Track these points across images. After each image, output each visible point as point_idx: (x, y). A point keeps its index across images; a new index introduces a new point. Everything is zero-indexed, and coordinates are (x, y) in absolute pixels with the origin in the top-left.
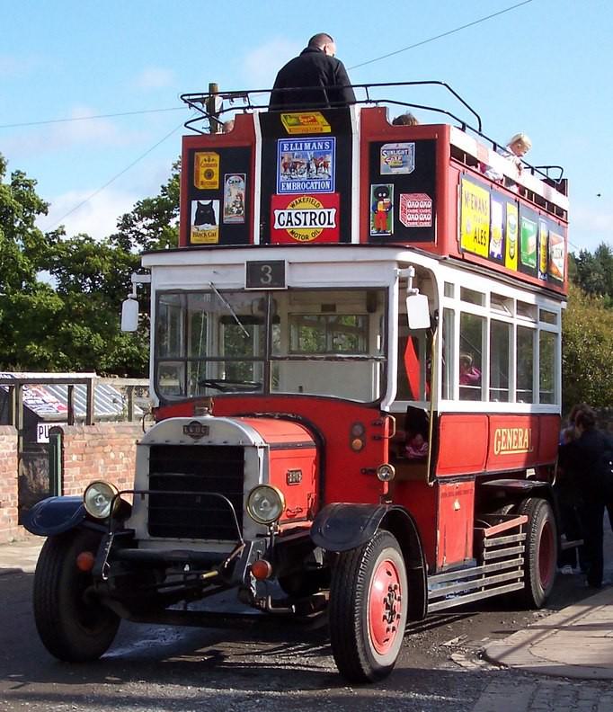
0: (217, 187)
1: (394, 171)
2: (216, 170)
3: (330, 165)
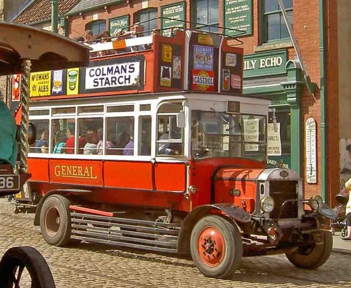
0: (171, 61)
1: (230, 65)
2: (171, 53)
3: (211, 59)
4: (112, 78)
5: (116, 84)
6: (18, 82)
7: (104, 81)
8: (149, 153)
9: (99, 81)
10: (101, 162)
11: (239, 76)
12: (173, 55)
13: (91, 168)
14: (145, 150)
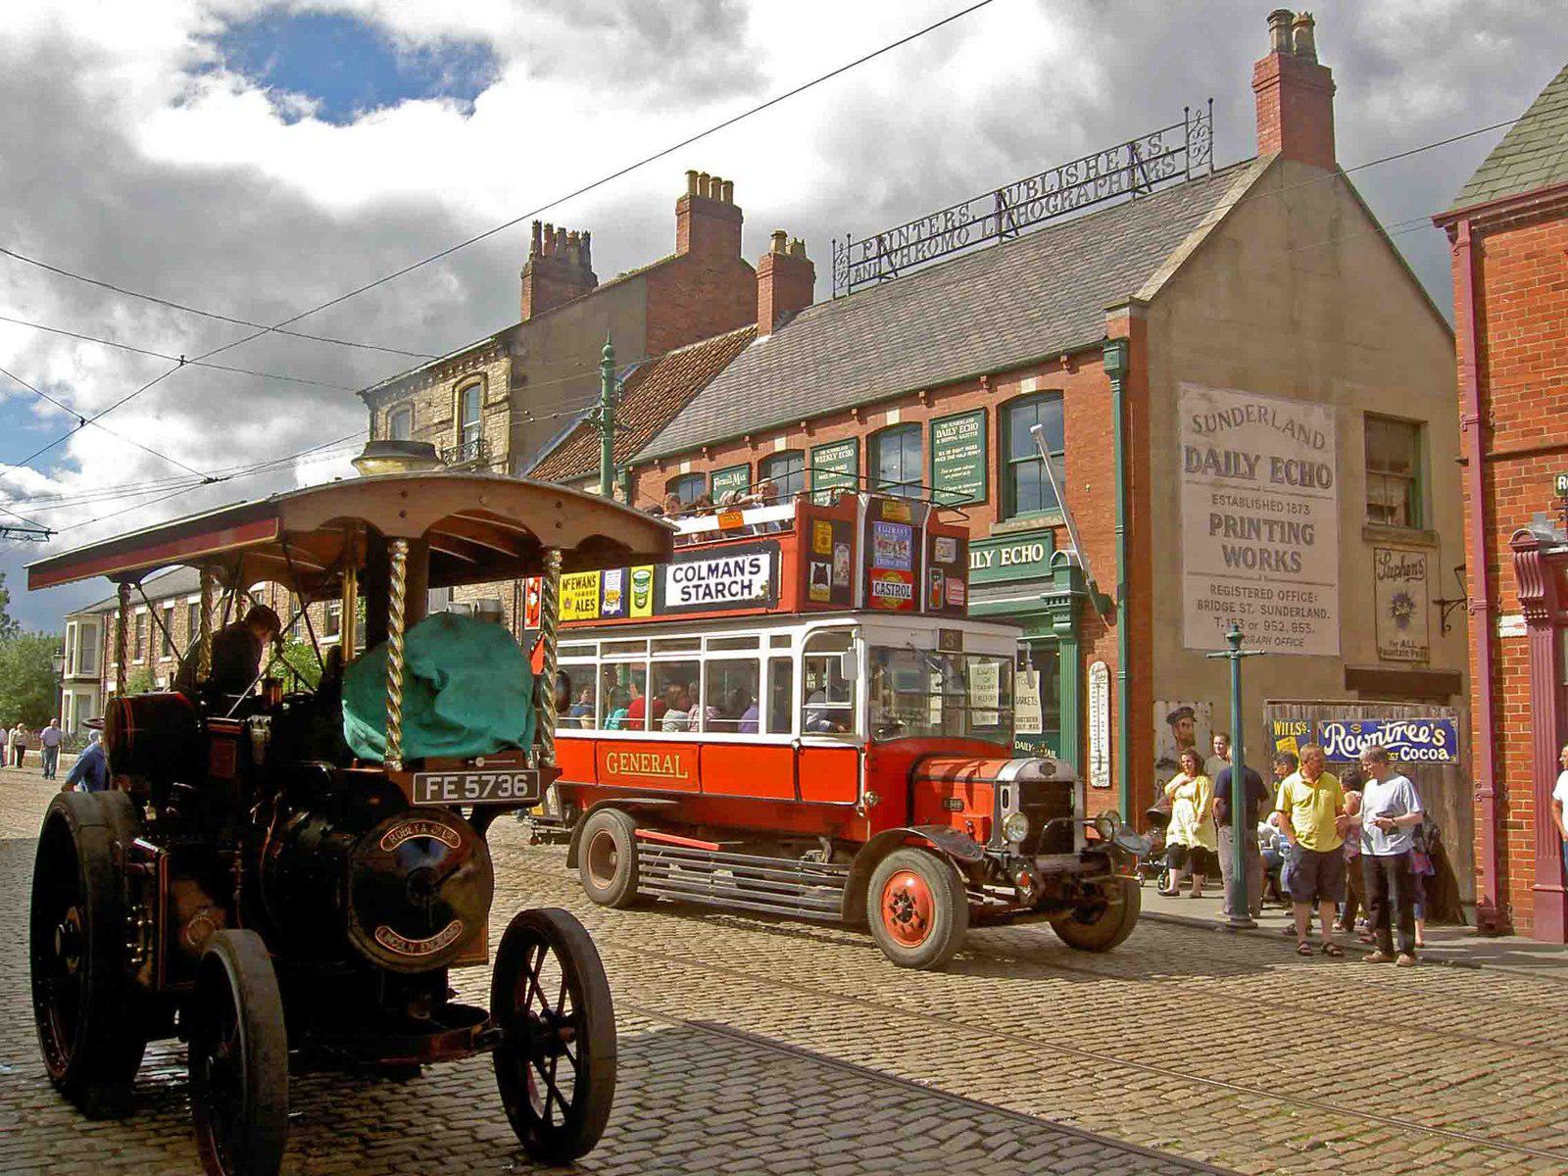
0: (829, 552)
1: (943, 560)
2: (829, 538)
4: (717, 584)
5: (724, 596)
6: (537, 593)
7: (701, 591)
8: (788, 730)
9: (693, 591)
10: (696, 747)
11: (960, 581)
12: (833, 541)
13: (677, 757)
14: (781, 723)
